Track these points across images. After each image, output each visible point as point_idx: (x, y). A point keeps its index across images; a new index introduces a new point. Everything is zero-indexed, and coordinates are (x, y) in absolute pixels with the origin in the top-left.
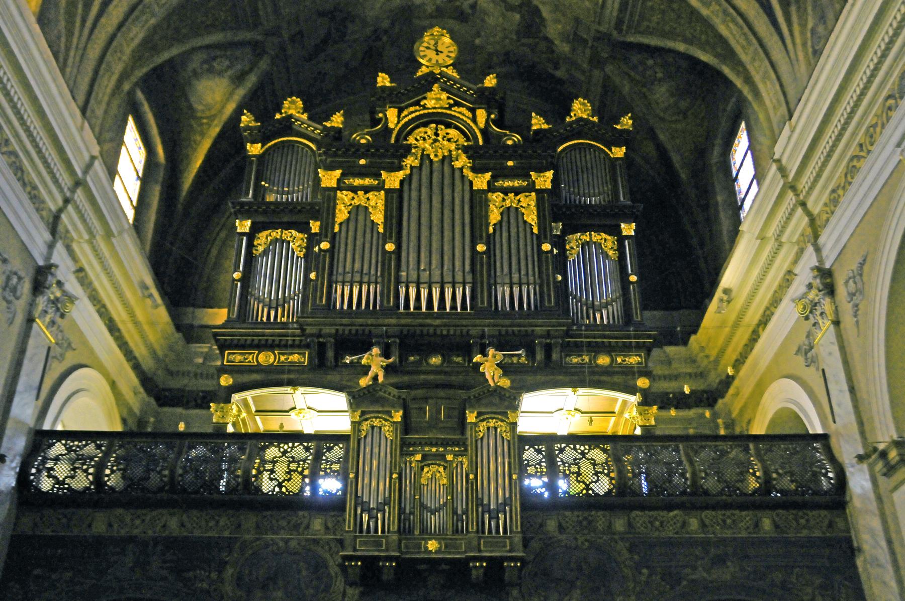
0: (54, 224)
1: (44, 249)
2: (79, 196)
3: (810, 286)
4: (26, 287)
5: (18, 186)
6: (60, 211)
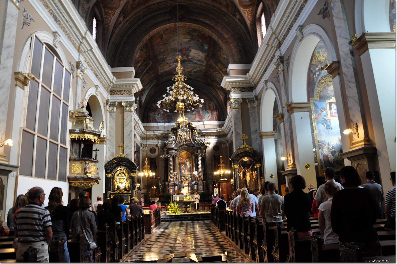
0: (79, 50)
1: (78, 57)
2: (84, 41)
3: (277, 60)
4: (75, 68)
5: (70, 42)
6: (80, 45)
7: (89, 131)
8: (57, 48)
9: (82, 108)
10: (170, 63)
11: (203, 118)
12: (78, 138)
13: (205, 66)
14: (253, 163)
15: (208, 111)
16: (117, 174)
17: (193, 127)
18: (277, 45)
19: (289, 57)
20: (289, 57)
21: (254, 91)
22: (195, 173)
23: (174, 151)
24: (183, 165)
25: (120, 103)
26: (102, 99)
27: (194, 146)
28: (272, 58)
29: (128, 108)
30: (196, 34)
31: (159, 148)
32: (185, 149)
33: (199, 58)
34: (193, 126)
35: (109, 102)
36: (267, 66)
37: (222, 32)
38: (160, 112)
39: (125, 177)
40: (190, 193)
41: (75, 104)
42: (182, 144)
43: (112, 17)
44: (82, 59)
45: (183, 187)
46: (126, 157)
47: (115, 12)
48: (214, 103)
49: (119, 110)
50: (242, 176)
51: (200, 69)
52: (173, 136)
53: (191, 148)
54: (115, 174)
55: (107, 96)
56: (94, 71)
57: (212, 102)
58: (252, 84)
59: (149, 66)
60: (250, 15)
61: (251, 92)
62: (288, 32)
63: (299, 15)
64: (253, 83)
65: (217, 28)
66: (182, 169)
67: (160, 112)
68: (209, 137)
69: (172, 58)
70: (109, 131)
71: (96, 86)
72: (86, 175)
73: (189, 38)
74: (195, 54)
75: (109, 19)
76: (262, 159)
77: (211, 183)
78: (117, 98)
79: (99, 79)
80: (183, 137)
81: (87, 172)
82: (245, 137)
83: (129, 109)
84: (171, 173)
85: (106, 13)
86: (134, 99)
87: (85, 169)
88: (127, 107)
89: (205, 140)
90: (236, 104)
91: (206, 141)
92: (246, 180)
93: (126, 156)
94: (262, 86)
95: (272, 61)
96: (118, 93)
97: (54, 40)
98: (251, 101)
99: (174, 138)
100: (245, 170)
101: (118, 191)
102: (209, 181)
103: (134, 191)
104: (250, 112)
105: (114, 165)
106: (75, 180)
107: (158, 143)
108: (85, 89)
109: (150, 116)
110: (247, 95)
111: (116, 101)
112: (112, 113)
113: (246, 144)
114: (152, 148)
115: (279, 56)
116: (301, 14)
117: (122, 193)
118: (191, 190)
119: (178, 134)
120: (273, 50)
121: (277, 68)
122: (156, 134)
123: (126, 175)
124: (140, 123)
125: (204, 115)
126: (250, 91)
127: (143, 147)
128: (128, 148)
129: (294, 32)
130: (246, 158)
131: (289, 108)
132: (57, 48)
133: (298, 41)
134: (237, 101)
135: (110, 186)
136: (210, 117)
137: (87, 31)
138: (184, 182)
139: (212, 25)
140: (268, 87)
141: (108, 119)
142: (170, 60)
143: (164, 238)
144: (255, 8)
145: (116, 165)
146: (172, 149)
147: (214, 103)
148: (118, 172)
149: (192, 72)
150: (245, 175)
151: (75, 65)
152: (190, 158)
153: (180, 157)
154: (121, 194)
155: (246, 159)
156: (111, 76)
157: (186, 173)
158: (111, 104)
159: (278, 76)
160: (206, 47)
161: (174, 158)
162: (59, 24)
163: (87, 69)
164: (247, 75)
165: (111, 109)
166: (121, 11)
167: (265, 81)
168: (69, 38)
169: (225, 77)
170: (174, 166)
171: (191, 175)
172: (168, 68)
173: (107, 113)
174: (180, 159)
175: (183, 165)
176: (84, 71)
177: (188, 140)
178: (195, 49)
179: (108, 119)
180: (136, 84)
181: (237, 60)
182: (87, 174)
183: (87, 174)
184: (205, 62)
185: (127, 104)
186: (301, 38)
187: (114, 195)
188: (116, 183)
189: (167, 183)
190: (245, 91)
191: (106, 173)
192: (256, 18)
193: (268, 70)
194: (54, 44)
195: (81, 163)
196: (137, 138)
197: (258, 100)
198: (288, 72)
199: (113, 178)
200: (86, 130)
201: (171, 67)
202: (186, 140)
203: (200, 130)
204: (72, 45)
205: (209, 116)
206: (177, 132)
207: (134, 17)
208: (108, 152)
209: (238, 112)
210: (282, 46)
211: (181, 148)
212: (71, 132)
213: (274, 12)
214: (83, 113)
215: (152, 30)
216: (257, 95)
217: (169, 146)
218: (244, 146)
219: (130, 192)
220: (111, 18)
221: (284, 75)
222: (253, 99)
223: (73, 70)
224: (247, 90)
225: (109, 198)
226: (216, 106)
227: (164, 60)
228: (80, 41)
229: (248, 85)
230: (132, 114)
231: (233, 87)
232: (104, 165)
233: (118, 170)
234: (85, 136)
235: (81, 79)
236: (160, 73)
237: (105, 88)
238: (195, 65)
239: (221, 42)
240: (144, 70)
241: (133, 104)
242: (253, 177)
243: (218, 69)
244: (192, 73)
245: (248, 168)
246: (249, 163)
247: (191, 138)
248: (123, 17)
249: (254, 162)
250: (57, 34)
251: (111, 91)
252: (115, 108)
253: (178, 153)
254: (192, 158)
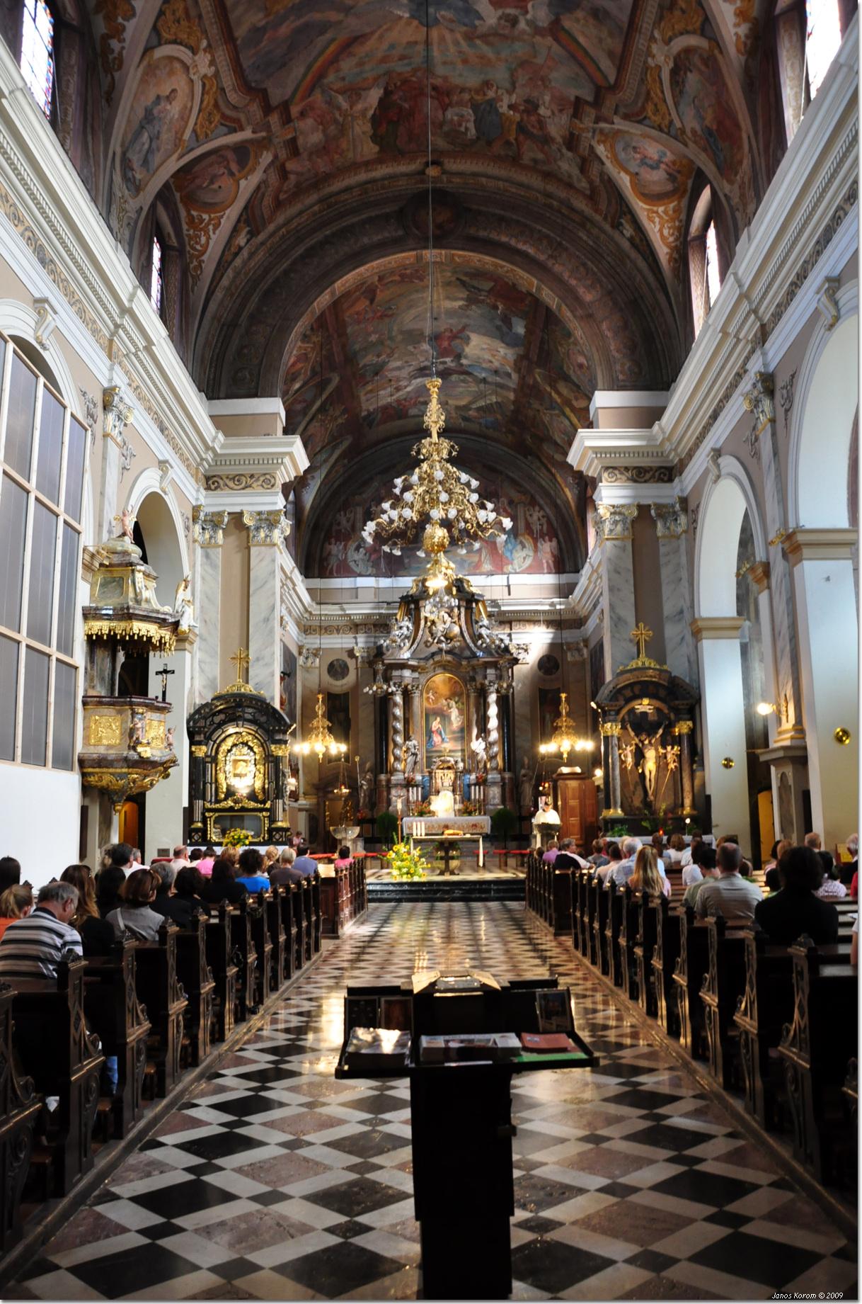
1: (107, 373)
2: (127, 321)
3: (754, 386)
5: (82, 326)
7: (145, 613)
8: (45, 349)
9: (120, 537)
10: (398, 380)
11: (508, 564)
12: (108, 635)
13: (515, 390)
14: (669, 719)
15: (521, 538)
16: (225, 747)
17: (473, 595)
18: (755, 335)
19: (793, 376)
20: (793, 376)
21: (677, 480)
22: (478, 746)
23: (407, 673)
24: (438, 719)
25: (237, 518)
26: (180, 505)
27: (474, 656)
28: (739, 376)
29: (262, 534)
30: (487, 285)
31: (360, 659)
32: (445, 667)
33: (496, 364)
34: (474, 590)
35: (202, 514)
36: (721, 401)
37: (573, 282)
39: (251, 757)
40: (459, 810)
41: (100, 526)
42: (434, 649)
43: (211, 233)
44: (120, 380)
45: (438, 792)
46: (254, 692)
47: (222, 217)
48: (542, 513)
49: (233, 540)
50: (630, 760)
51: (499, 400)
52: (407, 623)
53: (464, 663)
54: (219, 746)
55: (194, 493)
56: (156, 413)
57: (537, 508)
58: (671, 457)
59: (330, 388)
60: (669, 228)
61: (668, 485)
62: (791, 294)
63: (828, 241)
64: (673, 453)
65: (557, 268)
68: (524, 625)
69: (407, 362)
70: (202, 607)
71: (163, 465)
72: (134, 748)
73: (462, 299)
74: (483, 349)
75: (203, 240)
76: (697, 707)
77: (531, 779)
78: (229, 501)
79: (170, 440)
80: (440, 627)
81: (138, 742)
82: (645, 633)
83: (267, 536)
84: (396, 745)
85: (191, 221)
86: (279, 502)
87: (132, 732)
88: (258, 529)
89: (513, 636)
90: (616, 523)
91: (514, 642)
92: (643, 775)
93: (255, 689)
94: (704, 468)
95: (736, 387)
96: (231, 484)
97: (39, 324)
98: (665, 512)
99: (408, 628)
100: (640, 740)
101: (230, 803)
102: (523, 772)
103: (281, 801)
104: (662, 550)
105: (217, 719)
106: (100, 767)
107: (357, 643)
108: (129, 476)
109: (330, 554)
110: (654, 493)
111: (224, 512)
112: (209, 550)
113: (647, 656)
114: (337, 660)
115: (761, 374)
116: (836, 238)
117: (243, 809)
118: (462, 802)
119: (423, 614)
120: (742, 350)
121: (752, 411)
122: (349, 615)
123: (256, 749)
124: (297, 577)
125: (508, 554)
126: (663, 481)
127: (307, 658)
128: (261, 663)
129: (808, 298)
130: (646, 701)
131: (786, 545)
132: (45, 349)
133: (823, 330)
134: (620, 513)
135: (205, 784)
136: (528, 562)
137: (135, 288)
138: (439, 773)
139: (542, 257)
140: (723, 472)
141: (198, 568)
142: (399, 368)
143: (381, 953)
144: (685, 202)
145: (222, 716)
146: (403, 666)
147: (542, 513)
148: (230, 742)
149: (470, 409)
150: (639, 756)
151: (99, 399)
152: (460, 695)
153: (428, 693)
154: (238, 811)
155: (644, 706)
156: (208, 428)
157: (448, 746)
158: (208, 518)
159: (757, 439)
160: (520, 329)
161: (407, 695)
162: (52, 272)
163: (135, 411)
164: (656, 427)
165: (207, 536)
166: (241, 215)
167: (713, 450)
168: (81, 313)
169: (582, 432)
170: (407, 722)
171: (463, 751)
172: (391, 395)
173: (194, 550)
174: (428, 698)
175: (438, 719)
176: (126, 417)
177: (455, 636)
178: (484, 335)
179: (198, 568)
180: (290, 454)
181: (621, 377)
182: (139, 749)
183: (139, 749)
184: (515, 376)
185: (260, 520)
186: (829, 321)
187: (217, 814)
188: (221, 776)
189: (383, 777)
190: (645, 482)
191: (192, 743)
192: (689, 239)
193: (722, 415)
194: (37, 339)
195: (120, 712)
196: (288, 628)
197: (690, 512)
198: (787, 426)
199: (214, 760)
200: (134, 608)
201: (400, 393)
202: (448, 638)
203: (495, 603)
204: (88, 334)
205: (524, 558)
206: (418, 609)
207: (284, 230)
208: (197, 675)
209: (624, 549)
210: (771, 338)
211: (431, 662)
212: (89, 614)
213: (750, 223)
214: (125, 553)
215: (341, 277)
216: (685, 495)
217: (392, 654)
218: (640, 664)
219: (268, 805)
220: (209, 238)
221: (774, 434)
222: (673, 506)
223: (92, 417)
224: (653, 476)
225: (200, 825)
226: (549, 522)
227: (378, 370)
228: (111, 318)
229: (658, 459)
230: (275, 552)
231: (607, 468)
232: (185, 717)
233: (230, 735)
234: (131, 629)
235: (117, 444)
236: (364, 413)
237: (188, 467)
238: (482, 386)
239: (569, 314)
240: (313, 402)
241: (278, 522)
242: (667, 764)
243: (559, 400)
244: (471, 413)
245: (651, 733)
246: (656, 718)
247: (464, 628)
248: (249, 232)
249: (672, 716)
250: (46, 306)
251: (208, 479)
252: (221, 532)
253: (423, 680)
254: (468, 696)
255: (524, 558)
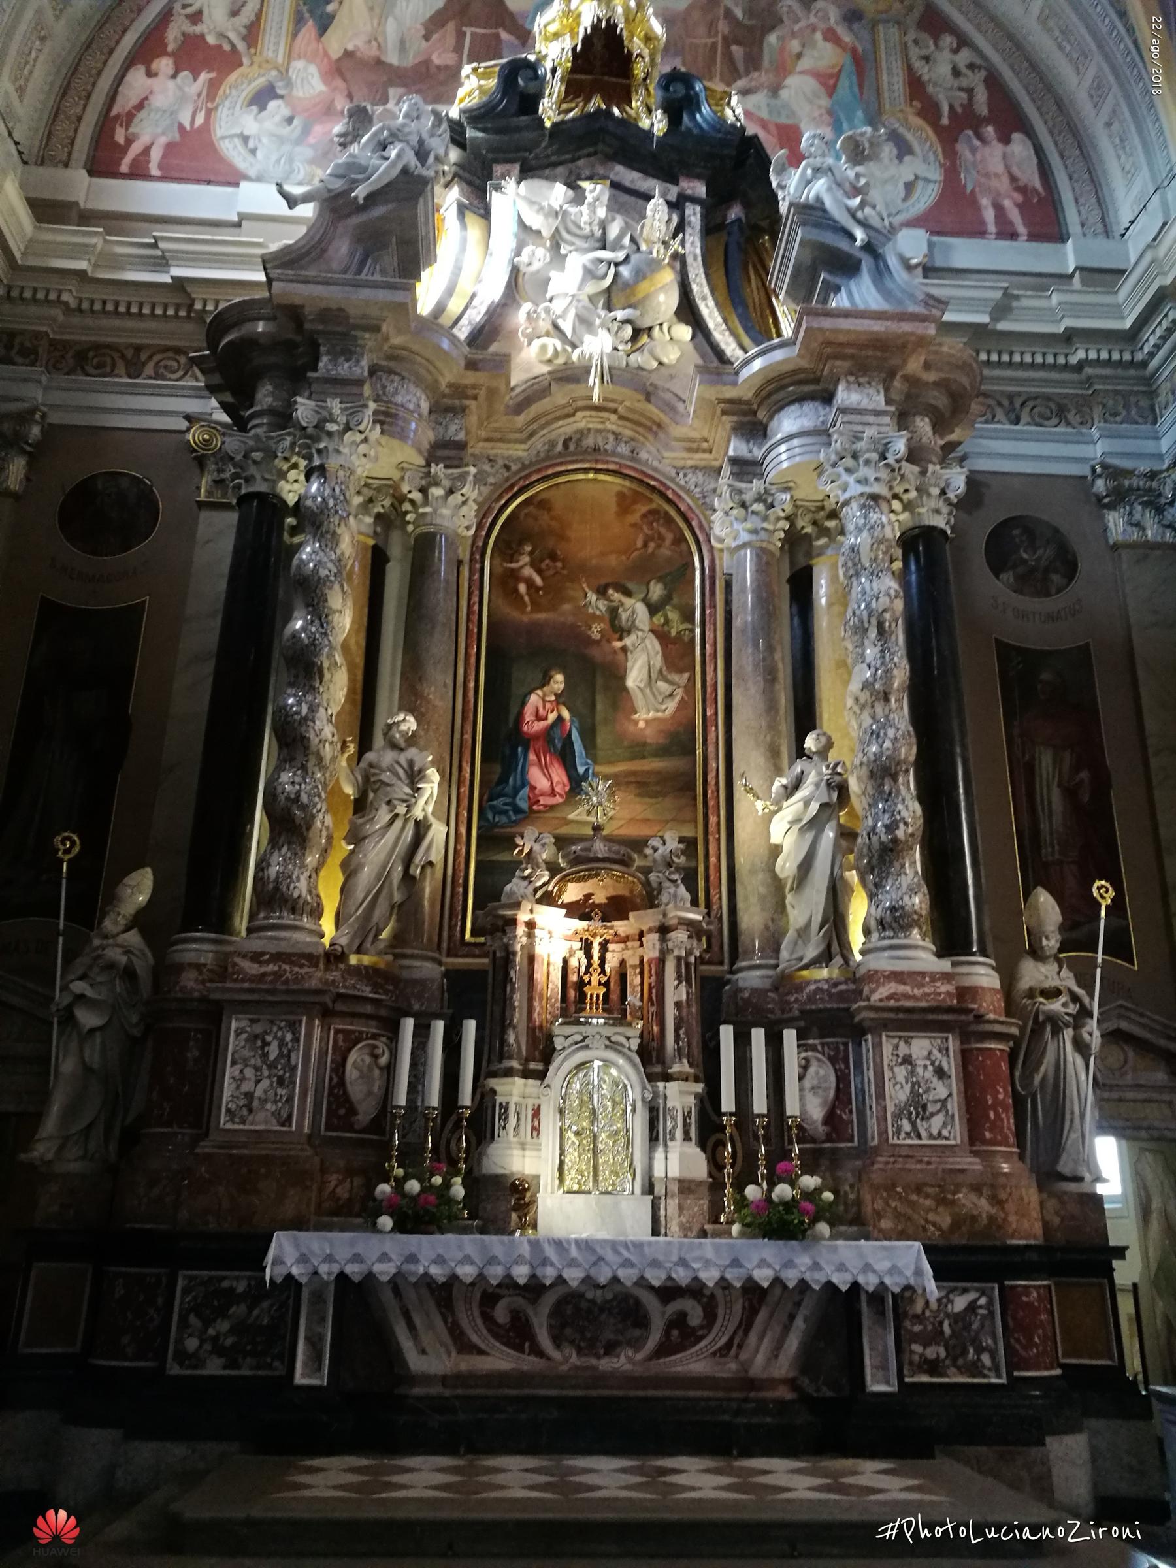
24: (558, 681)
38: (284, 73)
48: (964, 57)
66: (526, 742)
67: (289, 84)
175: (558, 681)
205: (909, 187)
226: (994, 82)
255: (909, 187)
